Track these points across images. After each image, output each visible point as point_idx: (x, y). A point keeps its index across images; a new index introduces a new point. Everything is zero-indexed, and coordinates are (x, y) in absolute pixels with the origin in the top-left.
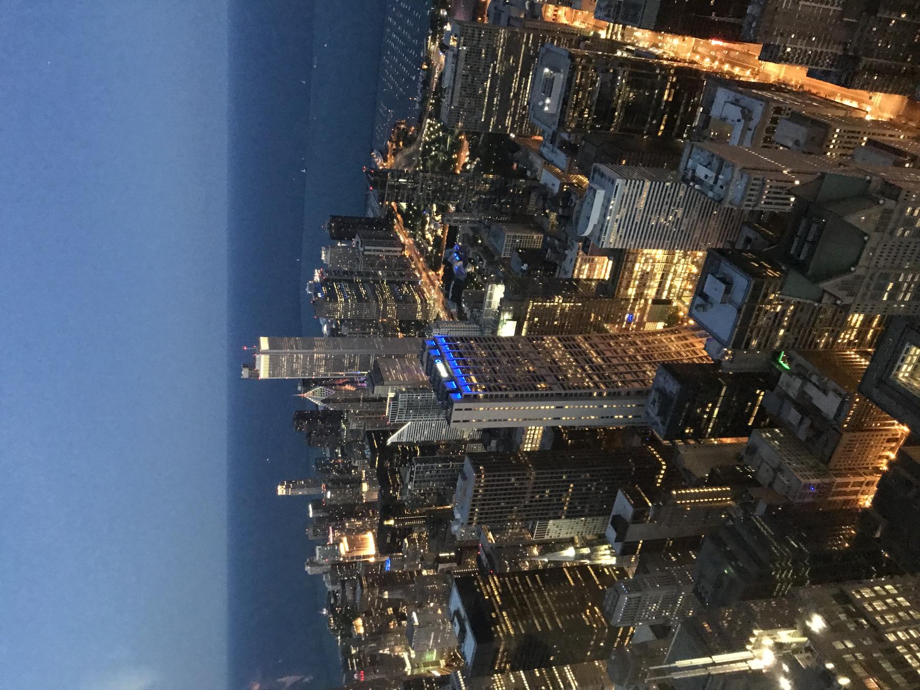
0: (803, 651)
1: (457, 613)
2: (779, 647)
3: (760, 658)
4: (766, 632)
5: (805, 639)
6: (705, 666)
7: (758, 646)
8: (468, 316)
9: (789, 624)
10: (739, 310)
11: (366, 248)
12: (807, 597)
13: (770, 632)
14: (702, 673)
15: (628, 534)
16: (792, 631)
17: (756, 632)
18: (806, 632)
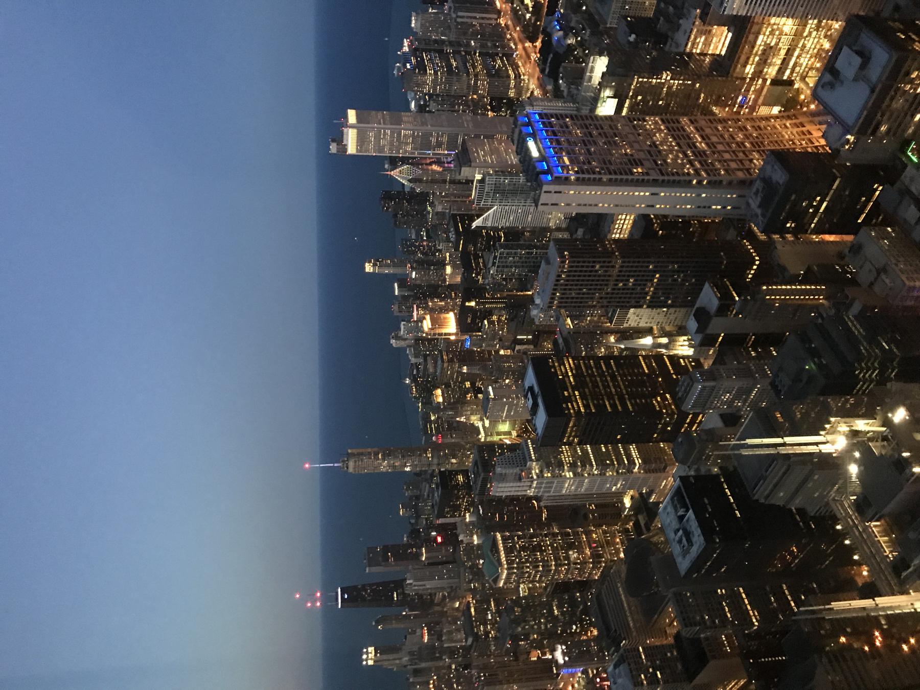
0: (880, 440)
1: (531, 389)
2: (855, 434)
3: (833, 443)
4: (844, 420)
5: (884, 429)
6: (775, 446)
7: (833, 431)
8: (565, 94)
10: (873, 91)
11: (460, 14)
12: (894, 389)
13: (847, 420)
14: (772, 451)
15: (711, 326)
17: (833, 419)
18: (887, 423)
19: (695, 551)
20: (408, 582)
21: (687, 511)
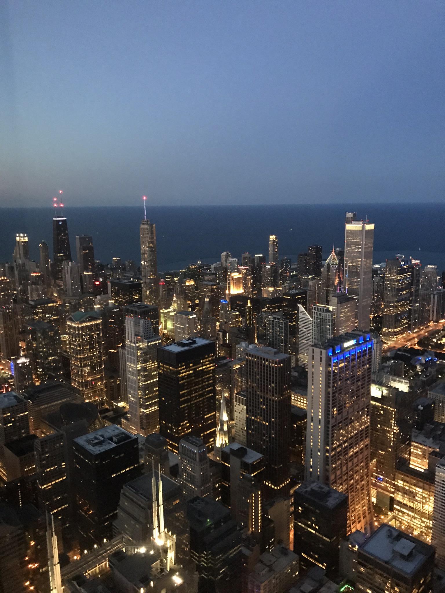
0: (161, 567)
1: (194, 342)
3: (159, 537)
4: (174, 544)
5: (168, 570)
7: (167, 537)
8: (384, 364)
9: (178, 560)
10: (386, 562)
11: (436, 296)
12: (194, 576)
13: (174, 546)
14: (154, 497)
15: (235, 458)
16: (173, 562)
17: (175, 537)
18: (172, 571)
19: (90, 448)
20: (70, 263)
21: (116, 443)
